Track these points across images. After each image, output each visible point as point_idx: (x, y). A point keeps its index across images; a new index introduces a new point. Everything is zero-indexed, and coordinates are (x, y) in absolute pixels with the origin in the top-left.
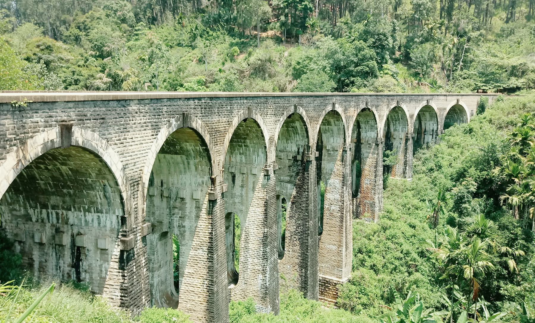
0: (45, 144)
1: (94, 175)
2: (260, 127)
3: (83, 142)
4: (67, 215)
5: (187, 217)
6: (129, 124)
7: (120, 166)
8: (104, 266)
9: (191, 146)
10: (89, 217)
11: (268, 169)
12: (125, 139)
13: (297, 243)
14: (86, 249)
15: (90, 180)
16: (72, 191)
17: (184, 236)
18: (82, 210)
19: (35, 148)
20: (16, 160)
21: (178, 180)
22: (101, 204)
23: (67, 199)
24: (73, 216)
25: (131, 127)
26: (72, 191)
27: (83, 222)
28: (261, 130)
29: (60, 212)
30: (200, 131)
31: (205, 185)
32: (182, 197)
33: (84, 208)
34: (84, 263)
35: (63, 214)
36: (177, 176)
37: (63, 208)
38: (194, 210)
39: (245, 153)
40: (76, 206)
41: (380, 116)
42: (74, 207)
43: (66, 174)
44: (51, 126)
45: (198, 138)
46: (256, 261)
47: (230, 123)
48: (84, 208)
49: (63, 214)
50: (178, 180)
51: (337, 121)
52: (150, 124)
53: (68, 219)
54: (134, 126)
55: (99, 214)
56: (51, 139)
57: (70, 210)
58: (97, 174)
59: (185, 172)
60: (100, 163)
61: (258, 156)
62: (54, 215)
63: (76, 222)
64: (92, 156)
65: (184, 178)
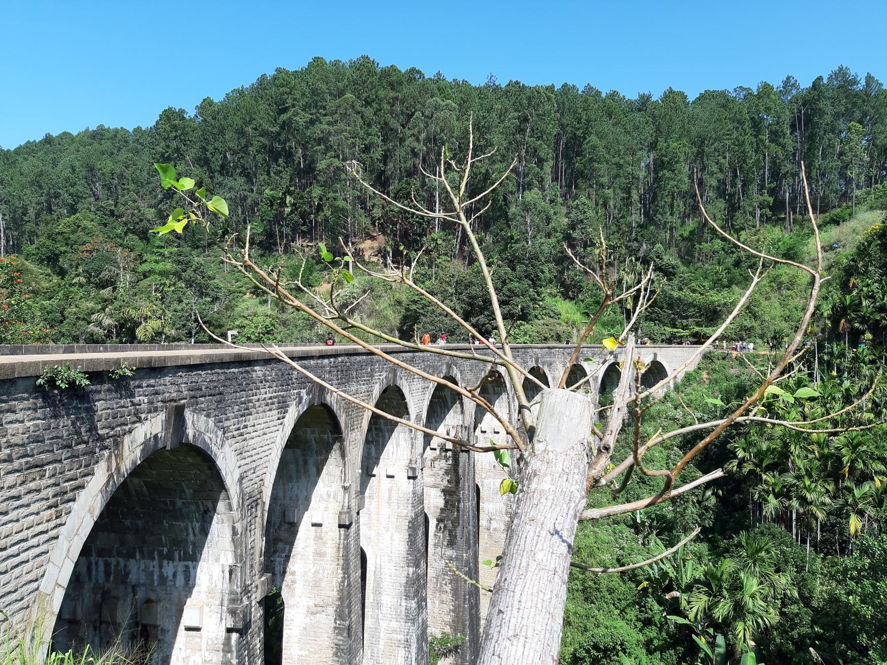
0: (145, 443)
1: (189, 492)
2: (404, 399)
3: (194, 436)
4: (125, 566)
5: (299, 556)
6: (250, 401)
7: (237, 477)
8: (191, 659)
9: (313, 433)
10: (169, 569)
11: (413, 466)
12: (246, 427)
13: (448, 588)
14: (159, 629)
15: (179, 503)
16: (140, 523)
17: (294, 590)
18: (156, 557)
19: (132, 452)
20: (107, 474)
21: (285, 492)
22: (194, 544)
23: (130, 537)
24: (136, 569)
25: (254, 407)
26: (140, 523)
27: (155, 577)
28: (406, 404)
29: (113, 561)
30: (335, 408)
31: (331, 500)
32: (291, 520)
33: (160, 553)
34: (155, 655)
35: (118, 564)
36: (284, 485)
37: (120, 554)
38: (312, 542)
39: (377, 442)
40: (145, 549)
41: (554, 378)
42: (141, 552)
43: (136, 491)
44: (156, 410)
45: (328, 421)
46: (394, 624)
47: (370, 392)
48: (160, 553)
49: (118, 564)
50: (285, 492)
51: (498, 386)
52: (276, 400)
53: (127, 574)
54: (258, 404)
55: (186, 563)
56: (154, 433)
57: (135, 557)
58: (195, 491)
59: (298, 478)
60: (208, 472)
61: (398, 445)
62: (102, 568)
63: (143, 578)
64: (198, 460)
65: (295, 488)
